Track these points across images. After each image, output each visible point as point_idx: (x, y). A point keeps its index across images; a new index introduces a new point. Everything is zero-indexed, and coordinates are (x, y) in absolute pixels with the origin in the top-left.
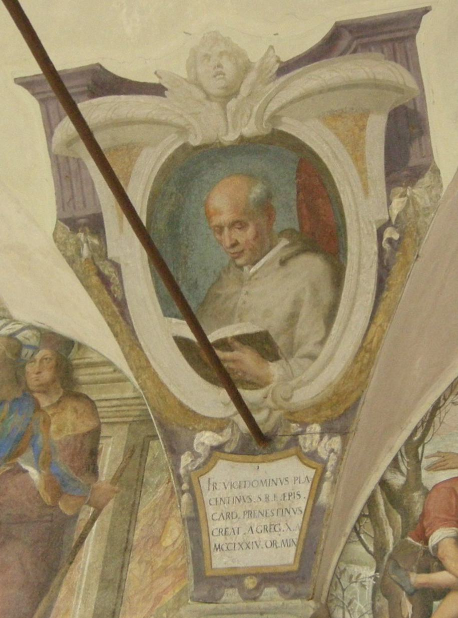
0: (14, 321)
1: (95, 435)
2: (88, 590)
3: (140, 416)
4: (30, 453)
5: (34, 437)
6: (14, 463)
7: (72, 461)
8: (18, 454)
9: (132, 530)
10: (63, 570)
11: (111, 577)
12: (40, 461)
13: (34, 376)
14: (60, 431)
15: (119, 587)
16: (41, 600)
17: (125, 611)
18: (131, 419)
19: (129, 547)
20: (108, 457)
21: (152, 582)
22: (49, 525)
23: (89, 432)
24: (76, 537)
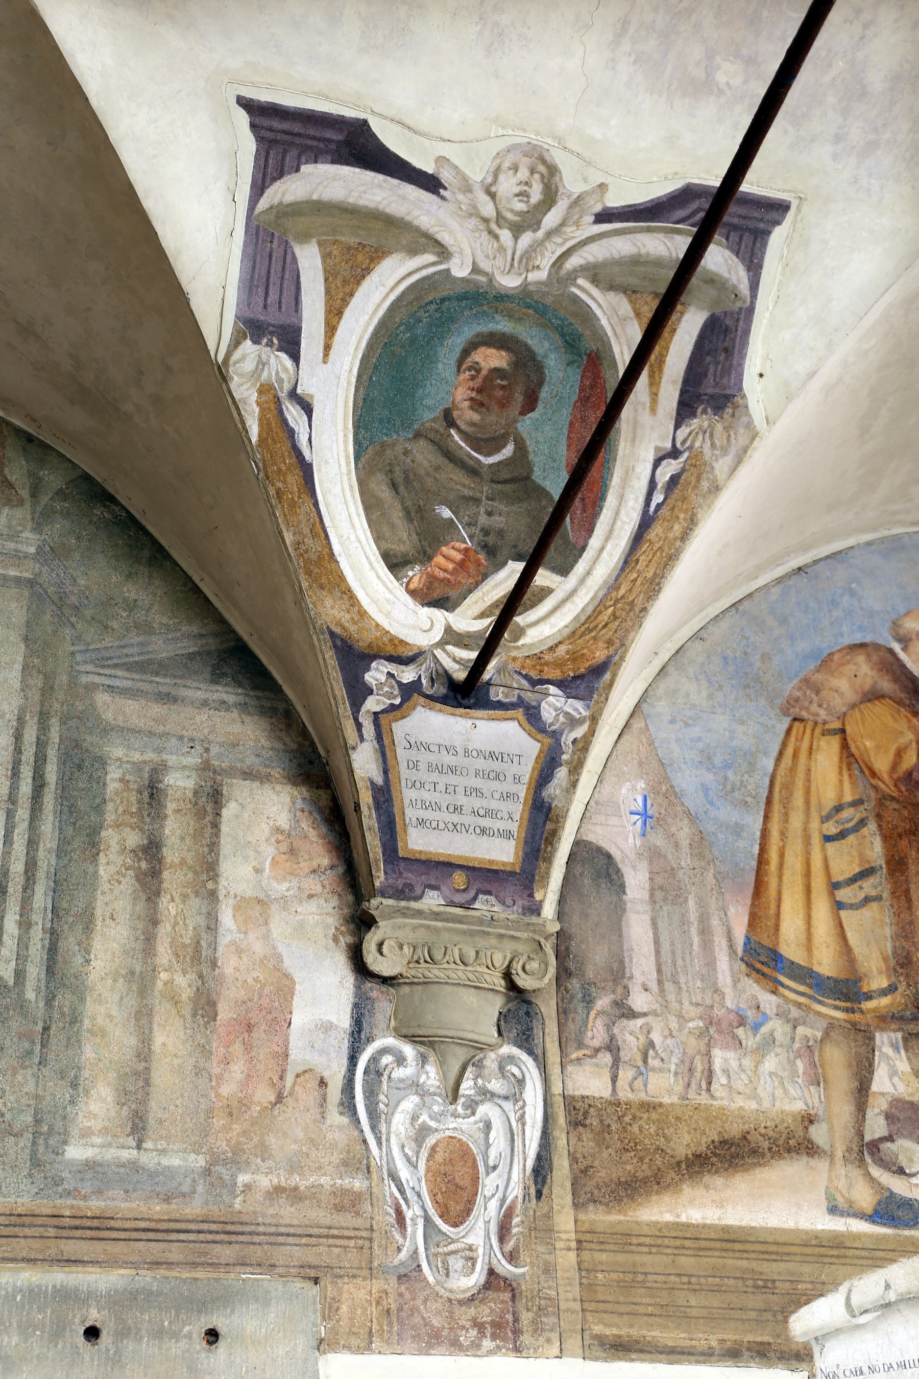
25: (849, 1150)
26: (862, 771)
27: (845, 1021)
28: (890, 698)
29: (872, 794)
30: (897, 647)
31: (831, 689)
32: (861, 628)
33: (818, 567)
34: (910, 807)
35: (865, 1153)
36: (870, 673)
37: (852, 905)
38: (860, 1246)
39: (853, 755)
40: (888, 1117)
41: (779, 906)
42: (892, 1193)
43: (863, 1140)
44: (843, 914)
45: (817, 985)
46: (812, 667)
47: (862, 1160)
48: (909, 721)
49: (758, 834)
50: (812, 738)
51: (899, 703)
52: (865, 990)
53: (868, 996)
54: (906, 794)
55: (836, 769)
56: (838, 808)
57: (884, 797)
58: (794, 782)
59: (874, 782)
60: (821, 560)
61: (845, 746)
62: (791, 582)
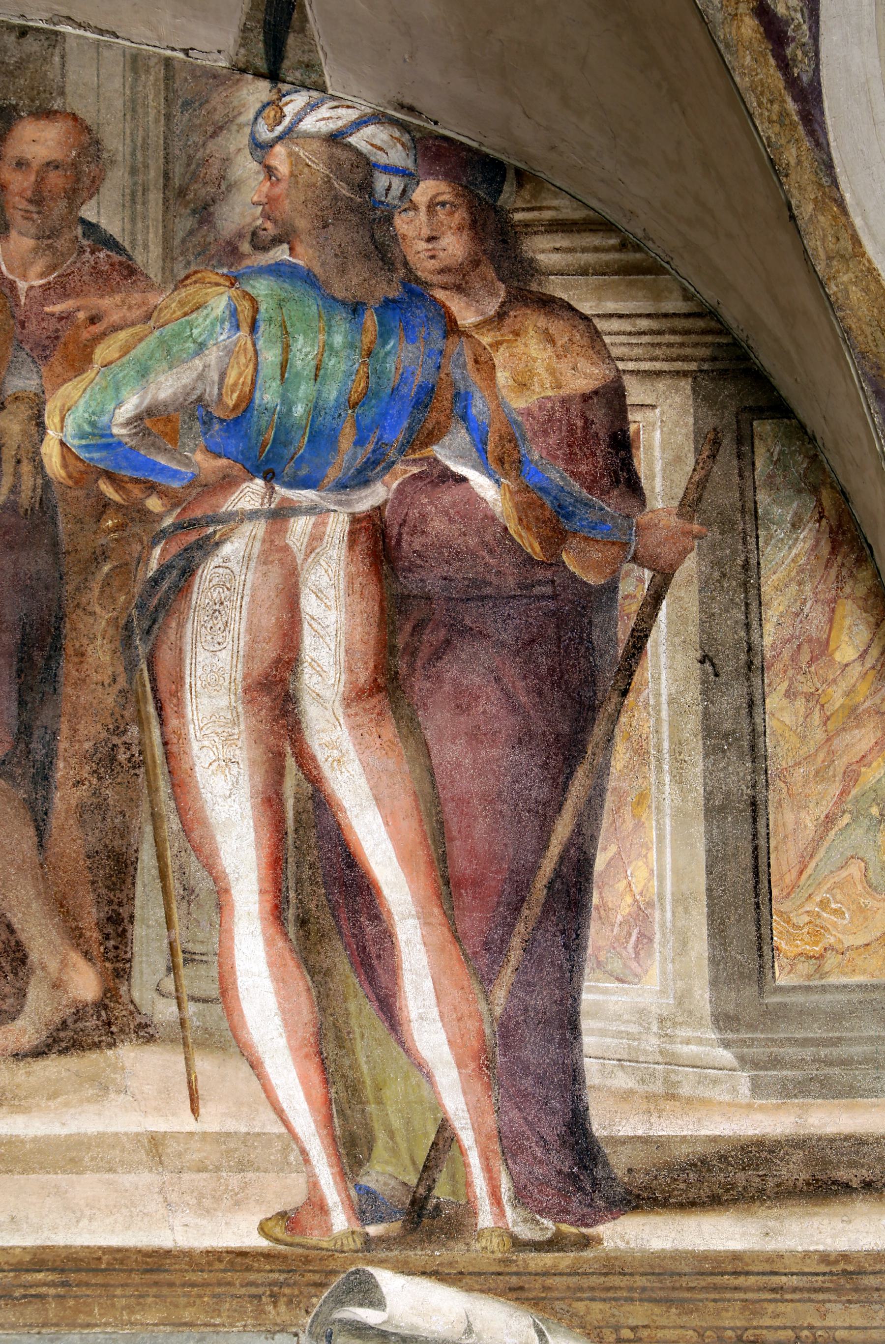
0: (333, 98)
2: (680, 753)
3: (714, 359)
4: (460, 436)
5: (462, 398)
6: (428, 458)
7: (571, 458)
8: (432, 437)
10: (610, 708)
11: (727, 726)
13: (423, 245)
14: (522, 386)
15: (753, 747)
16: (572, 773)
17: (779, 802)
18: (693, 366)
19: (757, 661)
20: (657, 453)
21: (828, 740)
22: (552, 605)
23: (596, 392)
24: (623, 633)
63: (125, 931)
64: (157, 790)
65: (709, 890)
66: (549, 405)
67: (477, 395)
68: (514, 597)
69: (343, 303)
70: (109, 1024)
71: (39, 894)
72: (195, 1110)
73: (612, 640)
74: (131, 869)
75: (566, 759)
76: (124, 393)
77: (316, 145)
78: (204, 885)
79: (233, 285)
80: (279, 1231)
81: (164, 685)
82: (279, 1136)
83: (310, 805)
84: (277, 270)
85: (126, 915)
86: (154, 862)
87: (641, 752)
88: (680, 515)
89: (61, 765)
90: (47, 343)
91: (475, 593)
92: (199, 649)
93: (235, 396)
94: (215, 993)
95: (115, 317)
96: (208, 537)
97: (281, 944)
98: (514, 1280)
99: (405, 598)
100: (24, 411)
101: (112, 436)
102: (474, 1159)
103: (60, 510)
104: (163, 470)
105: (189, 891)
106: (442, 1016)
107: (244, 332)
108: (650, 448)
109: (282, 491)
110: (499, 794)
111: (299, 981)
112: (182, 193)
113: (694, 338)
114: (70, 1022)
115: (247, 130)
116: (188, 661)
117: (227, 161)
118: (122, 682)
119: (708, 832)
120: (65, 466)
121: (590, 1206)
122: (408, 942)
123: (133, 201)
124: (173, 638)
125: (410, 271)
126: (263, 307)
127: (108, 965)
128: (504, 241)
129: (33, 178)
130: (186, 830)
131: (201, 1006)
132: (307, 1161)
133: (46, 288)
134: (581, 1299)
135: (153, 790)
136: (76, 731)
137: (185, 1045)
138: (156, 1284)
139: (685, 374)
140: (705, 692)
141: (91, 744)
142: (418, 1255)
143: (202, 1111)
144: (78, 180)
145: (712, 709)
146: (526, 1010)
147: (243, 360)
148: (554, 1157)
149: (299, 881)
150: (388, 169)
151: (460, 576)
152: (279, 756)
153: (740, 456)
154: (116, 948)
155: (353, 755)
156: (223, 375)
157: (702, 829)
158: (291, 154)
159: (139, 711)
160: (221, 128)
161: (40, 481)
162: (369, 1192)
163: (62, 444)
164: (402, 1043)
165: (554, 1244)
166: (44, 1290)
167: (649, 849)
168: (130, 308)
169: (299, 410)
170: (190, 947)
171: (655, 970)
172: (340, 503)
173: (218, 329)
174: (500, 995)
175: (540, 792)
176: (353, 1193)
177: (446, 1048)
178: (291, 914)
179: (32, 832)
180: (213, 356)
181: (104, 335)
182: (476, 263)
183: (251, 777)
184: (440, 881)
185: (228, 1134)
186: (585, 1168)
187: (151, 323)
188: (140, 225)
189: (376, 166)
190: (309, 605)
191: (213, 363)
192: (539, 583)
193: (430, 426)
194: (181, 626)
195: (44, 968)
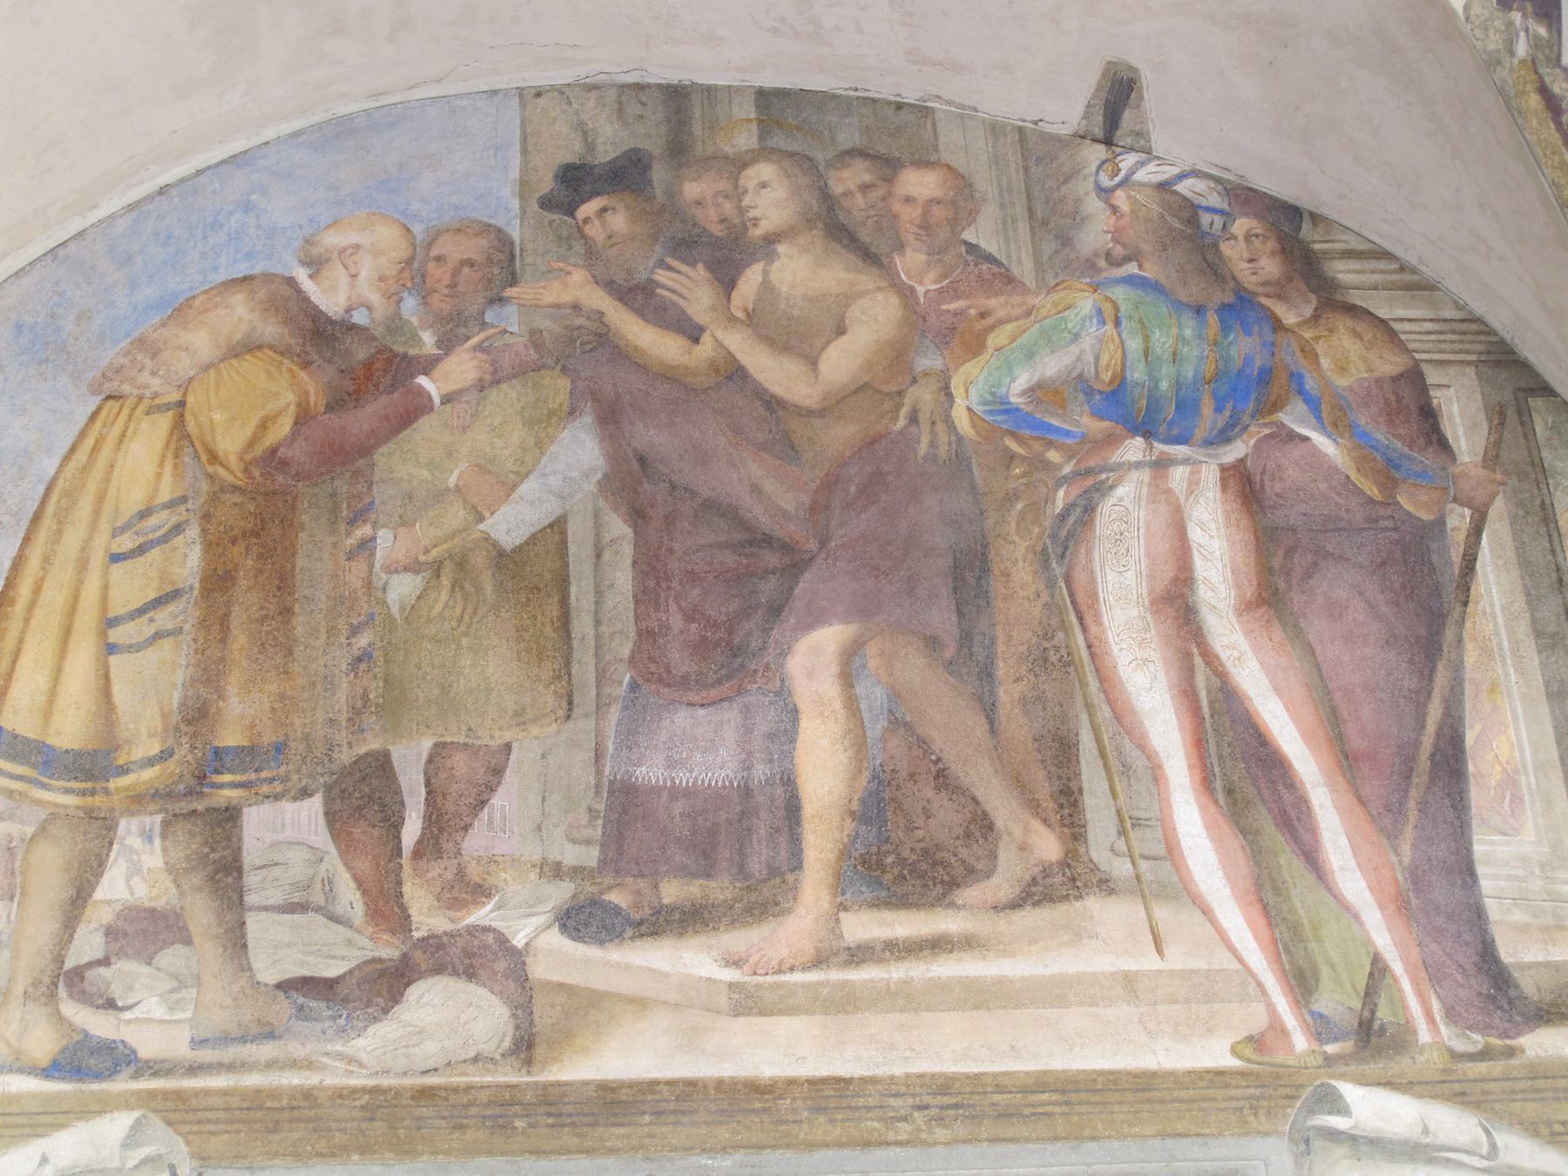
0: (1158, 158)
1: (1414, 378)
3: (1489, 353)
5: (1296, 379)
6: (1275, 423)
7: (1390, 423)
8: (1277, 406)
9: (1558, 550)
10: (1456, 615)
11: (1552, 629)
12: (1326, 424)
13: (1245, 265)
14: (1343, 369)
16: (1434, 667)
18: (1473, 357)
20: (1458, 421)
22: (1395, 535)
23: (1402, 375)
24: (1456, 555)
25: (36, 983)
26: (197, 457)
27: (78, 808)
28: (271, 348)
29: (205, 487)
30: (302, 275)
31: (179, 348)
32: (250, 256)
33: (202, 179)
34: (260, 499)
35: (61, 985)
36: (247, 316)
37: (131, 646)
38: (17, 1111)
39: (189, 436)
40: (111, 933)
41: (14, 662)
42: (87, 1034)
43: (61, 968)
44: (114, 660)
45: (46, 763)
46: (156, 319)
47: (52, 995)
48: (294, 376)
49: (8, 564)
50: (129, 420)
51: (284, 352)
52: (121, 762)
53: (124, 770)
54: (261, 480)
55: (157, 459)
56: (144, 514)
57: (222, 490)
58: (83, 485)
59: (210, 469)
60: (209, 168)
61: (179, 423)
62: (152, 207)
63: (1076, 801)
64: (1087, 684)
65: (1562, 759)
66: (1366, 384)
67: (1307, 376)
68: (1364, 529)
69: (1188, 306)
70: (1073, 880)
71: (996, 771)
72: (1160, 951)
73: (1449, 563)
74: (1074, 750)
75: (1427, 656)
76: (1016, 371)
77: (1149, 191)
78: (1139, 762)
79: (1096, 291)
80: (1249, 1053)
81: (1082, 599)
82: (1237, 971)
83: (1220, 696)
84: (1130, 280)
85: (1075, 788)
86: (1094, 744)
87: (1486, 651)
88: (1484, 467)
89: (1001, 664)
90: (946, 332)
91: (1331, 526)
92: (1108, 570)
93: (1110, 374)
94: (1162, 851)
95: (1001, 314)
96: (1103, 482)
97: (1213, 810)
98: (1457, 1087)
99: (1275, 529)
100: (934, 385)
101: (1010, 403)
102: (1406, 986)
103: (974, 461)
104: (1058, 430)
105: (1127, 769)
106: (1359, 865)
107: (1110, 327)
108: (1451, 417)
109: (1160, 447)
110: (1378, 684)
111: (1234, 841)
112: (1045, 223)
113: (1470, 337)
114: (1039, 879)
115: (1092, 179)
116: (1099, 580)
117: (1078, 200)
118: (1045, 597)
119: (1552, 712)
120: (973, 425)
121: (1509, 1021)
122: (1322, 806)
123: (1006, 229)
124: (1084, 562)
125: (1238, 283)
126: (1123, 308)
127: (1066, 830)
128: (1309, 264)
129: (919, 210)
130: (1118, 717)
131: (1152, 863)
132: (1264, 992)
133: (940, 291)
134: (1516, 1100)
135: (1084, 684)
136: (1010, 637)
137: (1143, 896)
138: (1149, 1101)
139: (1468, 363)
140: (1529, 603)
141: (1025, 647)
142: (1373, 1068)
143: (1166, 952)
144: (957, 213)
145: (1538, 615)
146: (1429, 860)
147: (1112, 347)
148: (1473, 981)
149: (1220, 758)
150: (1208, 209)
151: (1317, 512)
152: (1188, 656)
153: (1522, 424)
154: (1071, 815)
155: (1250, 654)
156: (1097, 359)
157: (1547, 710)
158: (1129, 197)
159: (1063, 621)
160: (1070, 177)
161: (954, 438)
162: (1321, 1016)
163: (969, 409)
164: (1329, 890)
165: (1484, 1055)
166: (1050, 1108)
167: (1507, 727)
168: (1013, 307)
169: (1164, 385)
170: (1135, 813)
171: (1530, 824)
172: (1209, 456)
173: (1088, 323)
174: (1406, 847)
175: (1410, 682)
176: (1308, 1018)
177: (1367, 894)
178: (1218, 785)
179: (982, 720)
180: (1087, 343)
181: (992, 328)
182: (1290, 279)
183: (1167, 674)
184: (1340, 755)
185: (1192, 971)
186: (1501, 989)
187: (1032, 318)
188: (1013, 246)
189: (1199, 206)
190: (1195, 535)
191: (1088, 349)
192: (1383, 518)
193: (1273, 397)
194: (1089, 551)
195: (1009, 834)
